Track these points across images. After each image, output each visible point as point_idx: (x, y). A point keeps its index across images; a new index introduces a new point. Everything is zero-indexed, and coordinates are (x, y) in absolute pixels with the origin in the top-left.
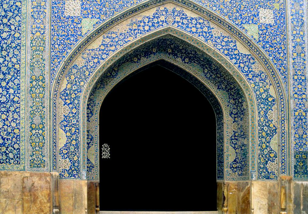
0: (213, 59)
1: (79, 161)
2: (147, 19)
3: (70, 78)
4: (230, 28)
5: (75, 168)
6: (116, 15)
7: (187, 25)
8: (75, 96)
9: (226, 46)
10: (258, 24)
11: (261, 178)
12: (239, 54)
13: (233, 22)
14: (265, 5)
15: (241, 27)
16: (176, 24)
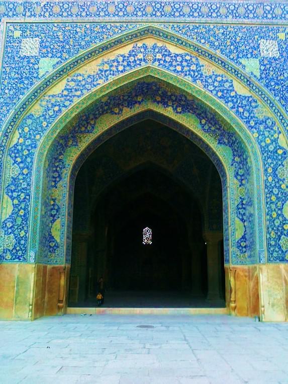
0: (206, 104)
1: (26, 237)
2: (122, 58)
3: (24, 131)
4: (223, 64)
5: (20, 247)
6: (82, 53)
7: (170, 63)
8: (27, 152)
9: (219, 87)
10: (259, 58)
11: (272, 259)
12: (236, 96)
13: (226, 57)
14: (267, 35)
15: (237, 62)
16: (157, 63)
